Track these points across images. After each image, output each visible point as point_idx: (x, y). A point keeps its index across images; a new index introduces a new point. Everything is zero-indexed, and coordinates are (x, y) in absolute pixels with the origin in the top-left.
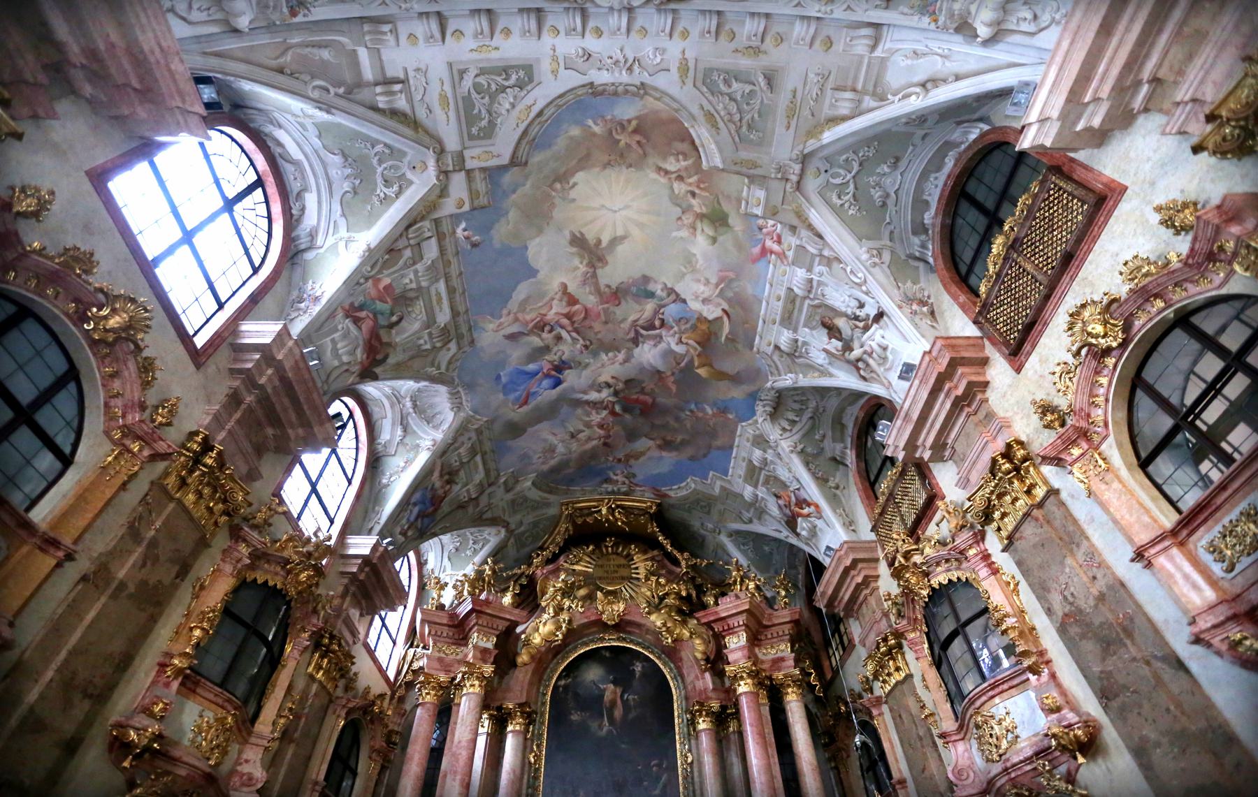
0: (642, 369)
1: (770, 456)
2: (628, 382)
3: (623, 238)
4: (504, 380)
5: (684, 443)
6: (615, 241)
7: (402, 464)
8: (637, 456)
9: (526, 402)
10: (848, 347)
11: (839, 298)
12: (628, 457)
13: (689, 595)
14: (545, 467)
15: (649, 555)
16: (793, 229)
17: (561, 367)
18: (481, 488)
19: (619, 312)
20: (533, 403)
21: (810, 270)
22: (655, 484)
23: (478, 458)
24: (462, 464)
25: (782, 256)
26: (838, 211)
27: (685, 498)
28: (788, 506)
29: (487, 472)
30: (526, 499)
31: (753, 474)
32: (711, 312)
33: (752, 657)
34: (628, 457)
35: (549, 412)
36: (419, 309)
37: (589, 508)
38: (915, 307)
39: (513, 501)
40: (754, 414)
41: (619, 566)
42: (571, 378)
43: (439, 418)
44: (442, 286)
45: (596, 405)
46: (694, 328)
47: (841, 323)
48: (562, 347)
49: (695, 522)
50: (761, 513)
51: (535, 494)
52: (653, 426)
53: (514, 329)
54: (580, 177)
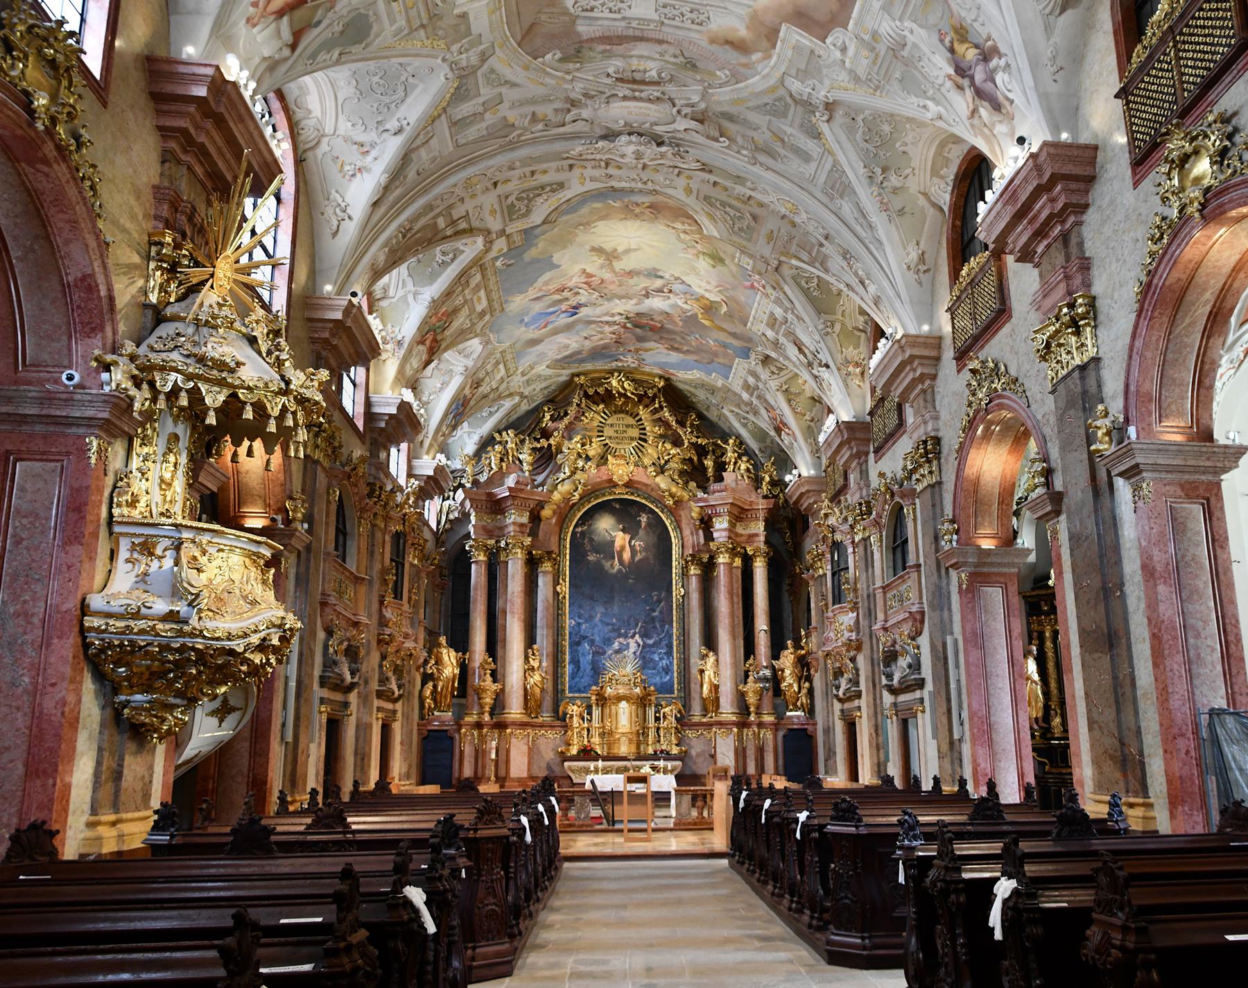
0: (652, 310)
1: (761, 385)
2: (637, 314)
3: (635, 250)
4: (526, 320)
5: (688, 351)
6: (628, 251)
7: (439, 385)
8: (647, 350)
9: (545, 327)
10: (810, 365)
11: (805, 339)
12: (637, 350)
13: (691, 460)
14: (559, 357)
15: (657, 416)
16: (774, 288)
17: (577, 307)
18: (502, 380)
19: (631, 282)
20: (550, 327)
21: (786, 312)
22: (661, 366)
23: (501, 366)
24: (487, 374)
25: (767, 295)
26: (806, 292)
27: (692, 380)
28: (775, 419)
29: (507, 370)
30: (540, 376)
31: (747, 387)
32: (713, 297)
33: (731, 529)
34: (637, 350)
35: (568, 328)
36: (465, 312)
37: (600, 379)
38: (851, 369)
39: (528, 381)
40: (748, 357)
41: (627, 426)
42: (583, 312)
43: (469, 350)
44: (482, 293)
45: (607, 323)
46: (698, 300)
47: (806, 351)
48: (578, 297)
49: (701, 395)
50: (756, 413)
51: (550, 372)
52: (661, 338)
53: (539, 294)
54: (600, 224)
